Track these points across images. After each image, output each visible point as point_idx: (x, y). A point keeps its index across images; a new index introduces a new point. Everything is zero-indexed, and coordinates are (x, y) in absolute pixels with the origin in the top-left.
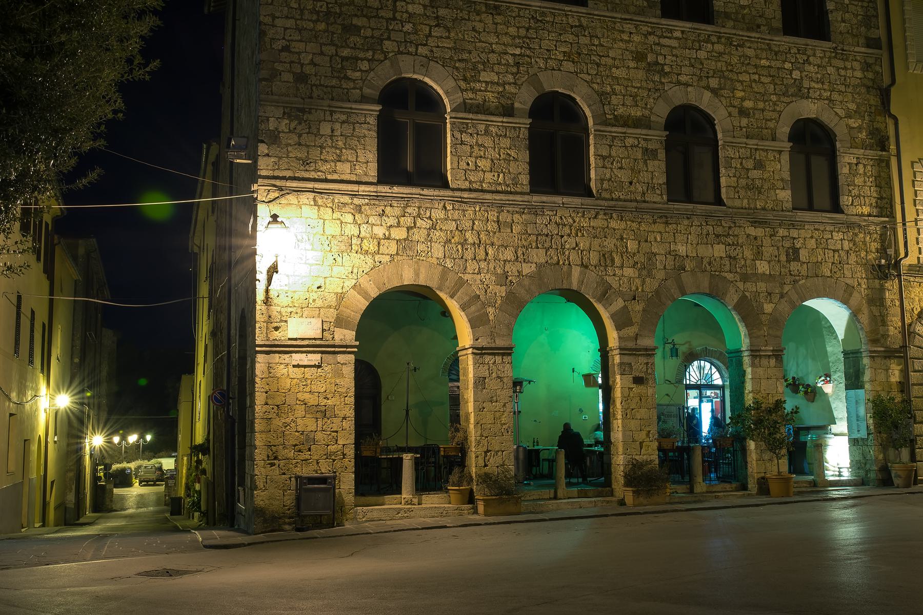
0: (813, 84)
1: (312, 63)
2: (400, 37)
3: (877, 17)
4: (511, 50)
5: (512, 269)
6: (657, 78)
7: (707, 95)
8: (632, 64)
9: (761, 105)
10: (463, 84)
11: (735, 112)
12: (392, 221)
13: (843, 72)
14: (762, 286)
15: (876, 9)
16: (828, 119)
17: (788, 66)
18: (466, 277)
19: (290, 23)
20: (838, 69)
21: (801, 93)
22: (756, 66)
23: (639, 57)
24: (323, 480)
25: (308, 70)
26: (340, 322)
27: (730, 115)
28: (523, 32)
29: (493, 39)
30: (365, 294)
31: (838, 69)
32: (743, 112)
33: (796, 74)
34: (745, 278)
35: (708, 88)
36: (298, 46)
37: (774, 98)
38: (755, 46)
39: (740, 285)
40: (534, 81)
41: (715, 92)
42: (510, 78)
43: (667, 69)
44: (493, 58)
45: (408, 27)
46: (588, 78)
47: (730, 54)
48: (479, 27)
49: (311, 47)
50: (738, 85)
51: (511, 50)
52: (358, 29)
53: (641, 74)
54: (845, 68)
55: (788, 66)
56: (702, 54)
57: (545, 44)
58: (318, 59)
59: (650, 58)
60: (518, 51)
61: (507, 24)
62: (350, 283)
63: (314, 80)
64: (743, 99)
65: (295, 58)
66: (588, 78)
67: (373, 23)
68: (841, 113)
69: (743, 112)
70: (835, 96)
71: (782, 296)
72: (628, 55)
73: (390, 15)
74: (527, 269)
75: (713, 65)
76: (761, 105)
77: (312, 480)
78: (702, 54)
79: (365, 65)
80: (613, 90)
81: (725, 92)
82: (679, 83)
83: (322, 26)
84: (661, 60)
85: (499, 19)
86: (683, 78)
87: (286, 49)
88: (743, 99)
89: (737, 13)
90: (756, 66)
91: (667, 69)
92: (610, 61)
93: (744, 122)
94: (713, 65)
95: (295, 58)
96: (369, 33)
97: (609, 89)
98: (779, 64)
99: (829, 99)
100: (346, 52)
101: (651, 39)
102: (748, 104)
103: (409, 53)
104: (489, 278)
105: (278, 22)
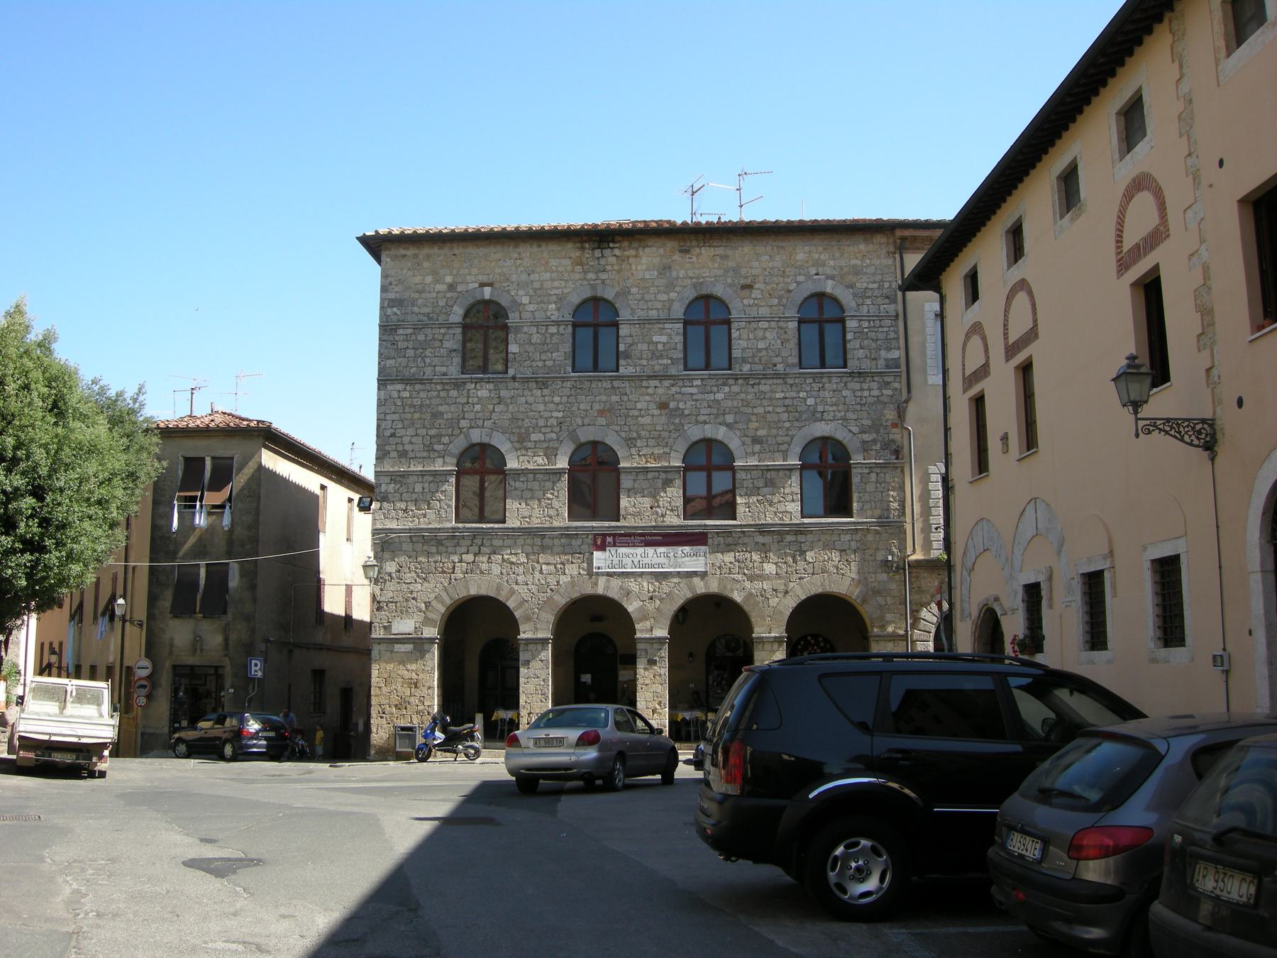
0: (827, 408)
1: (411, 443)
2: (472, 416)
3: (898, 339)
4: (555, 414)
5: (552, 580)
6: (677, 421)
7: (723, 429)
8: (656, 412)
9: (774, 431)
10: (518, 446)
11: (748, 441)
12: (464, 549)
13: (858, 394)
14: (766, 585)
15: (896, 332)
16: (840, 435)
17: (802, 395)
18: (516, 587)
19: (396, 417)
20: (854, 391)
21: (816, 416)
22: (771, 399)
23: (663, 406)
24: (410, 729)
25: (408, 447)
26: (427, 622)
27: (744, 444)
28: (565, 399)
29: (542, 407)
30: (443, 603)
31: (854, 391)
32: (756, 440)
33: (810, 401)
34: (751, 578)
35: (723, 423)
36: (400, 432)
37: (787, 425)
38: (771, 382)
39: (747, 584)
40: (573, 436)
41: (729, 426)
42: (554, 436)
43: (687, 412)
44: (541, 422)
45: (478, 407)
46: (618, 428)
47: (747, 393)
48: (531, 399)
49: (411, 431)
50: (754, 418)
51: (555, 414)
52: (442, 414)
53: (663, 419)
54: (862, 390)
55: (802, 395)
56: (720, 396)
57: (582, 406)
58: (414, 440)
59: (672, 405)
60: (561, 415)
61: (553, 394)
62: (432, 596)
63: (411, 455)
64: (756, 430)
65: (399, 440)
66: (618, 428)
67: (453, 408)
68: (855, 429)
69: (756, 440)
70: (850, 415)
71: (786, 592)
72: (652, 406)
73: (465, 400)
74: (564, 579)
75: (729, 403)
76: (774, 431)
77: (403, 729)
78: (720, 396)
79: (445, 440)
80: (640, 437)
81: (740, 426)
82: (697, 422)
83: (417, 415)
84: (681, 405)
85: (546, 392)
86: (701, 418)
87: (393, 435)
88: (756, 430)
89: (754, 356)
90: (771, 399)
91: (687, 412)
92: (637, 413)
93: (757, 448)
94: (729, 403)
95: (399, 440)
96: (449, 416)
97: (635, 435)
98: (793, 394)
99: (844, 419)
100: (432, 432)
101: (674, 389)
102: (761, 433)
103: (478, 427)
104: (534, 588)
105: (388, 417)
